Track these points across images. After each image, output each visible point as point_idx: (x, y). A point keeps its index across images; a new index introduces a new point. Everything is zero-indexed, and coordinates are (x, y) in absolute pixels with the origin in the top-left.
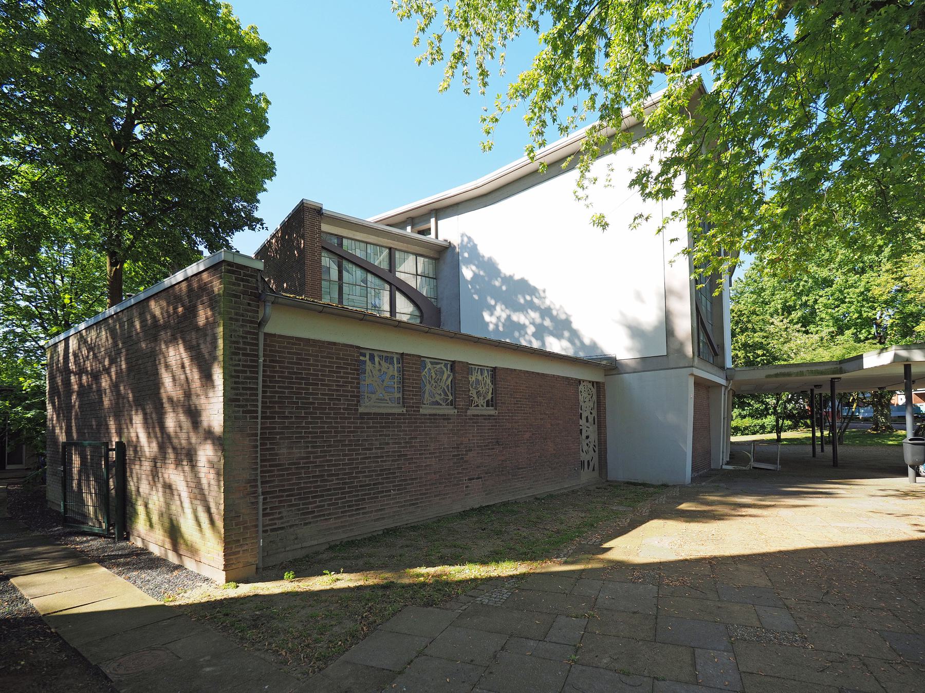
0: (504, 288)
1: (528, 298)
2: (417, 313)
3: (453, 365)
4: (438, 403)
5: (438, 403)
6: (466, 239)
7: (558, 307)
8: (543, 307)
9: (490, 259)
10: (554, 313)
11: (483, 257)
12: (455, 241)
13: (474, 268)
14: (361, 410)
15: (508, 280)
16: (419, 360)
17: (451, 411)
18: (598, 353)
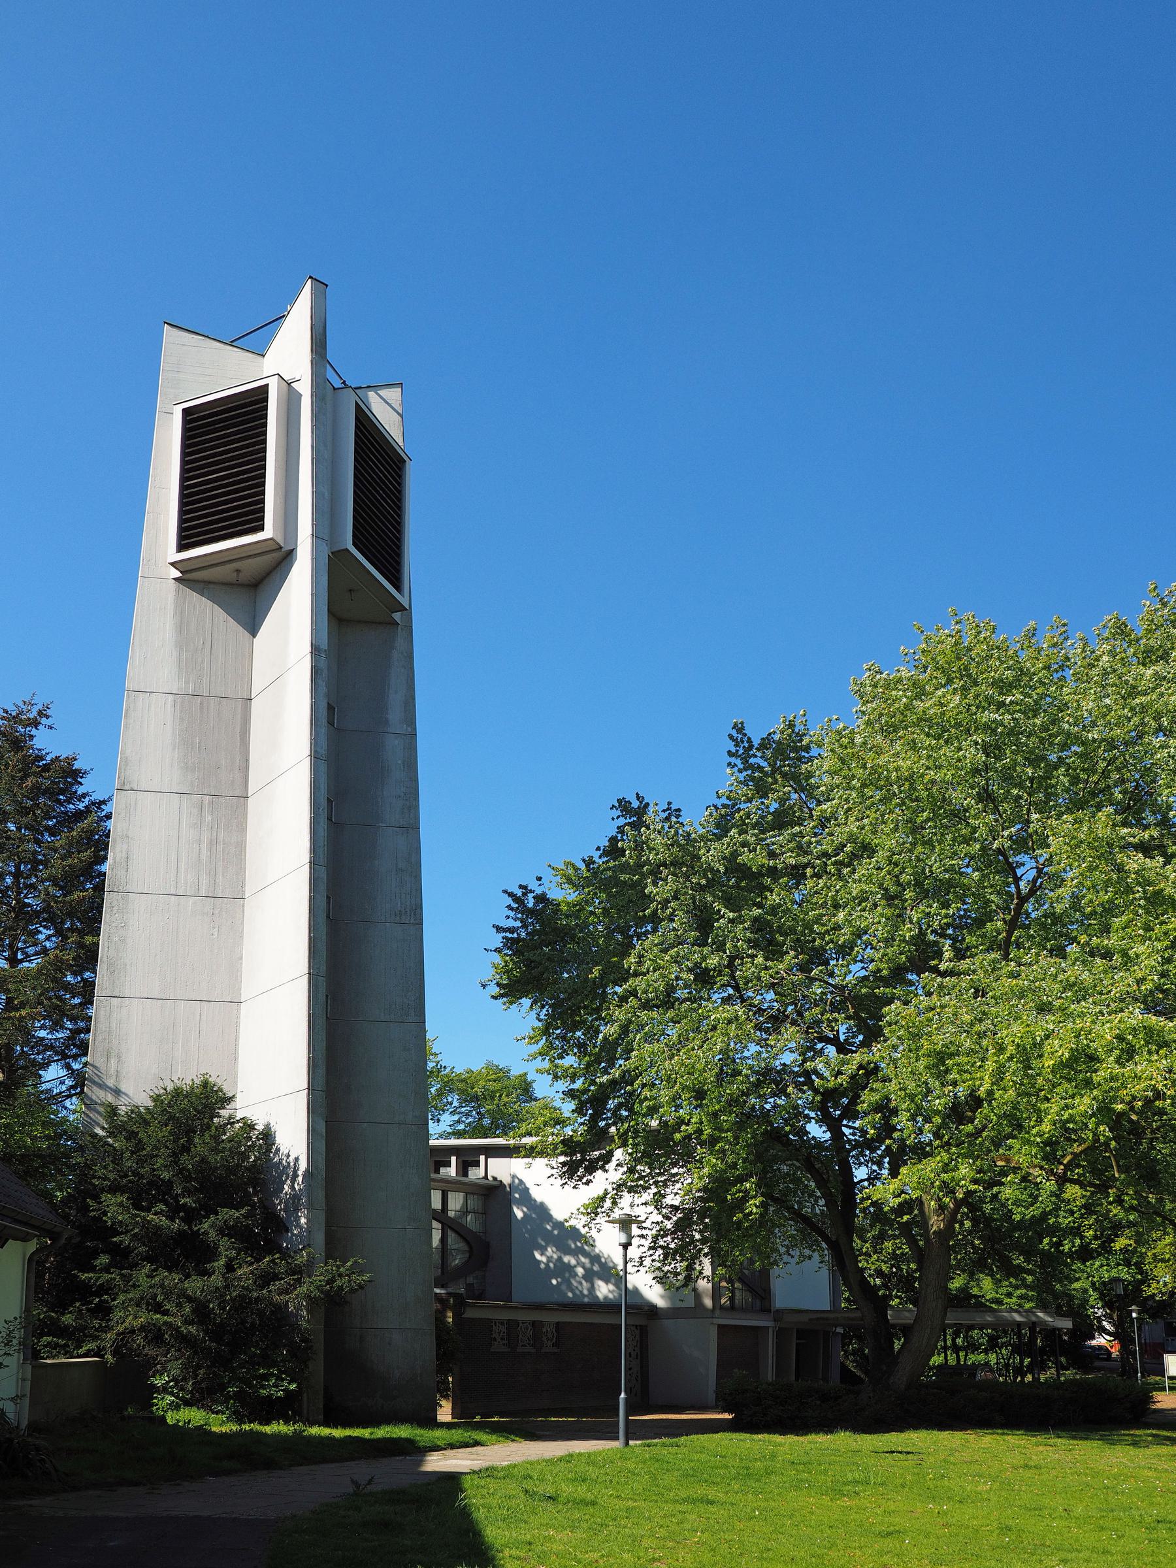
0: (556, 1232)
1: (579, 1244)
2: (466, 1248)
3: (534, 1323)
4: (525, 1346)
5: (525, 1346)
6: (517, 1181)
7: (606, 1256)
8: (592, 1254)
9: (542, 1204)
10: (603, 1260)
11: (535, 1201)
12: (506, 1180)
13: (525, 1209)
14: (492, 1350)
15: (559, 1225)
16: (517, 1322)
17: (533, 1351)
18: (639, 1301)
